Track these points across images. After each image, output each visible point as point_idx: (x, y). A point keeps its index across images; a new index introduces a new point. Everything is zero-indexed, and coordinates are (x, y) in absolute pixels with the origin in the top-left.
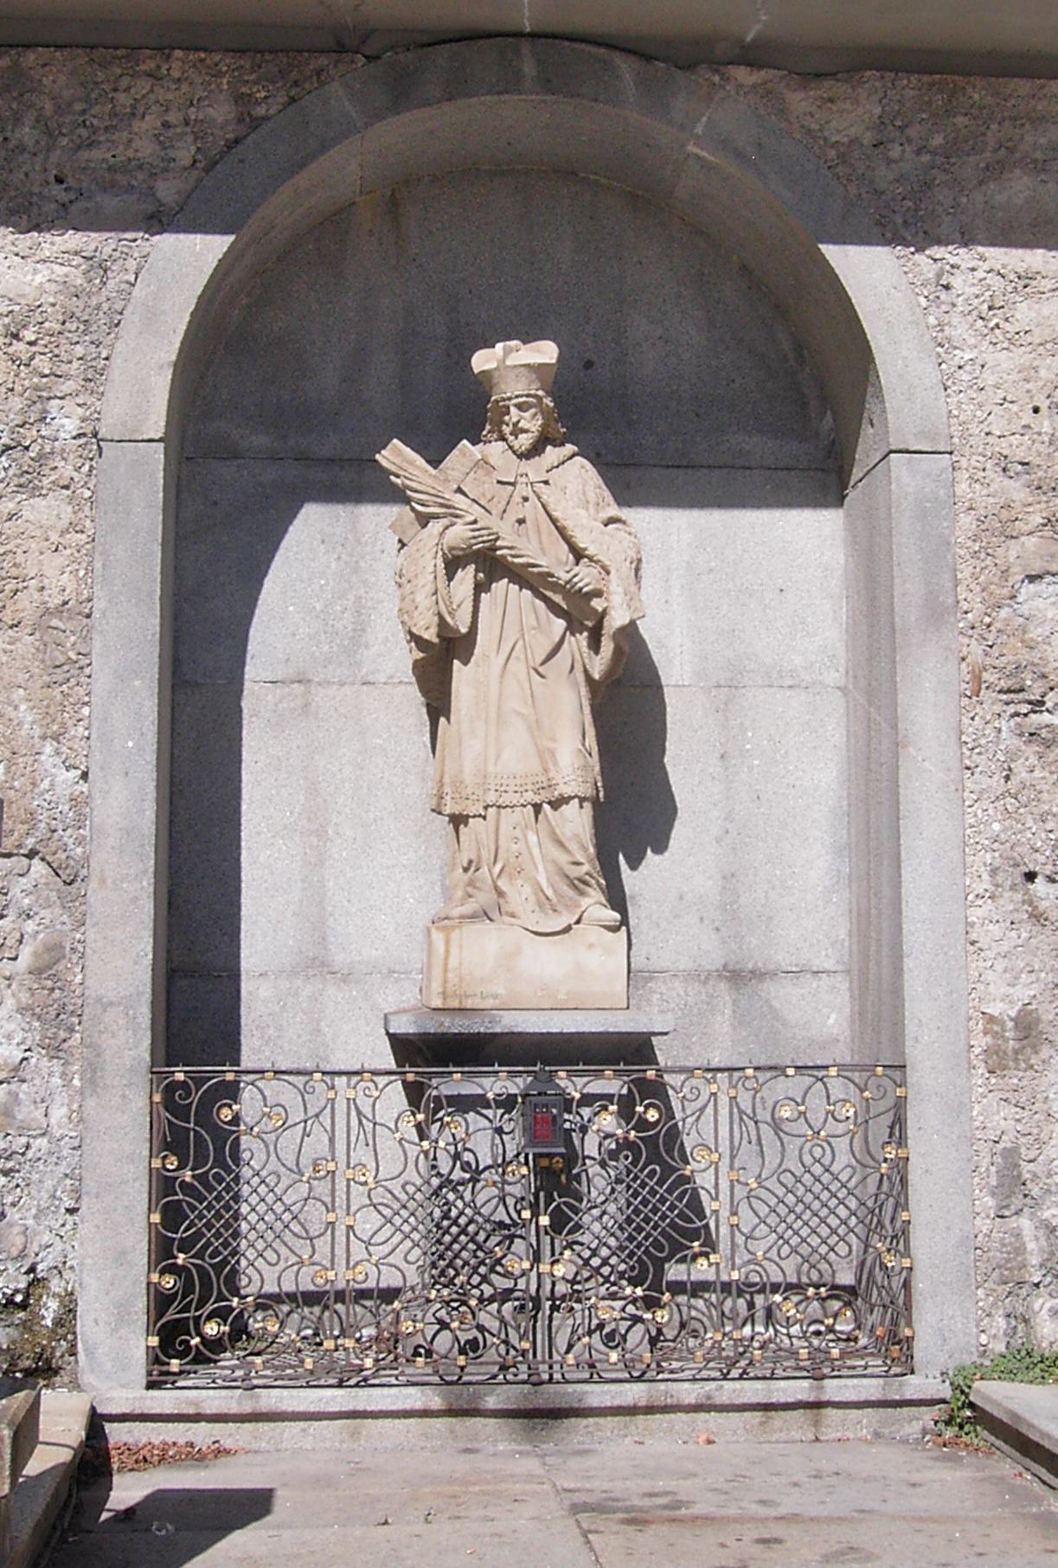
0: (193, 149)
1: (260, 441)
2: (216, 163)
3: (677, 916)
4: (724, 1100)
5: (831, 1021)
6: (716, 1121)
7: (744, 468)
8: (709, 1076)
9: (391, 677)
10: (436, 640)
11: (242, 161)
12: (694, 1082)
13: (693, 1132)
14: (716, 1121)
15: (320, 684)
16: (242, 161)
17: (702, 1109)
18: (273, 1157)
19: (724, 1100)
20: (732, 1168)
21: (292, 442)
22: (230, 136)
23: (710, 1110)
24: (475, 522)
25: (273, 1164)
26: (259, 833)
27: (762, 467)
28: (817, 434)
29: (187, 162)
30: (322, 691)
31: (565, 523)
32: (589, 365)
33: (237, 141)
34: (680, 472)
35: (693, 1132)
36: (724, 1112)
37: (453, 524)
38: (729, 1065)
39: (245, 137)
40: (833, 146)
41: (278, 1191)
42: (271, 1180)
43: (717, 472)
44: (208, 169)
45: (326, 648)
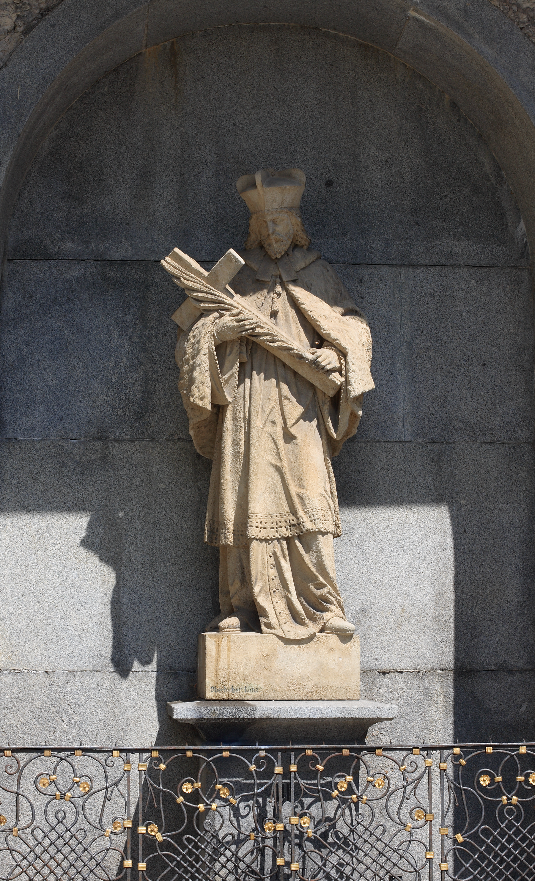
0: (14, 16)
1: (70, 246)
2: (33, 28)
3: (400, 625)
4: (436, 772)
5: (523, 709)
6: (430, 788)
7: (455, 266)
8: (425, 753)
9: (173, 435)
10: (209, 407)
11: (53, 26)
12: (412, 757)
13: (412, 797)
14: (430, 788)
15: (116, 441)
16: (53, 26)
17: (419, 779)
18: (81, 817)
19: (436, 772)
20: (442, 825)
21: (92, 246)
22: (43, 6)
23: (425, 779)
24: (238, 315)
25: (81, 822)
26: (67, 560)
27: (469, 266)
28: (513, 239)
29: (9, 27)
30: (117, 447)
31: (214, 671)
32: (329, 183)
33: (49, 10)
34: (403, 270)
35: (412, 797)
36: (436, 781)
37: (221, 316)
38: (442, 744)
39: (55, 6)
40: (525, 11)
41: (85, 843)
42: (80, 835)
43: (433, 269)
44: (25, 33)
45: (120, 412)
